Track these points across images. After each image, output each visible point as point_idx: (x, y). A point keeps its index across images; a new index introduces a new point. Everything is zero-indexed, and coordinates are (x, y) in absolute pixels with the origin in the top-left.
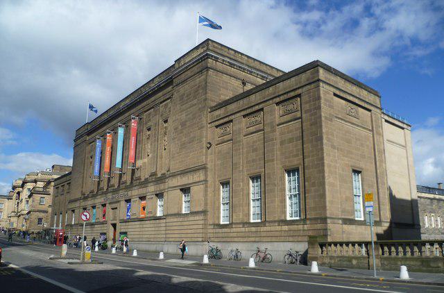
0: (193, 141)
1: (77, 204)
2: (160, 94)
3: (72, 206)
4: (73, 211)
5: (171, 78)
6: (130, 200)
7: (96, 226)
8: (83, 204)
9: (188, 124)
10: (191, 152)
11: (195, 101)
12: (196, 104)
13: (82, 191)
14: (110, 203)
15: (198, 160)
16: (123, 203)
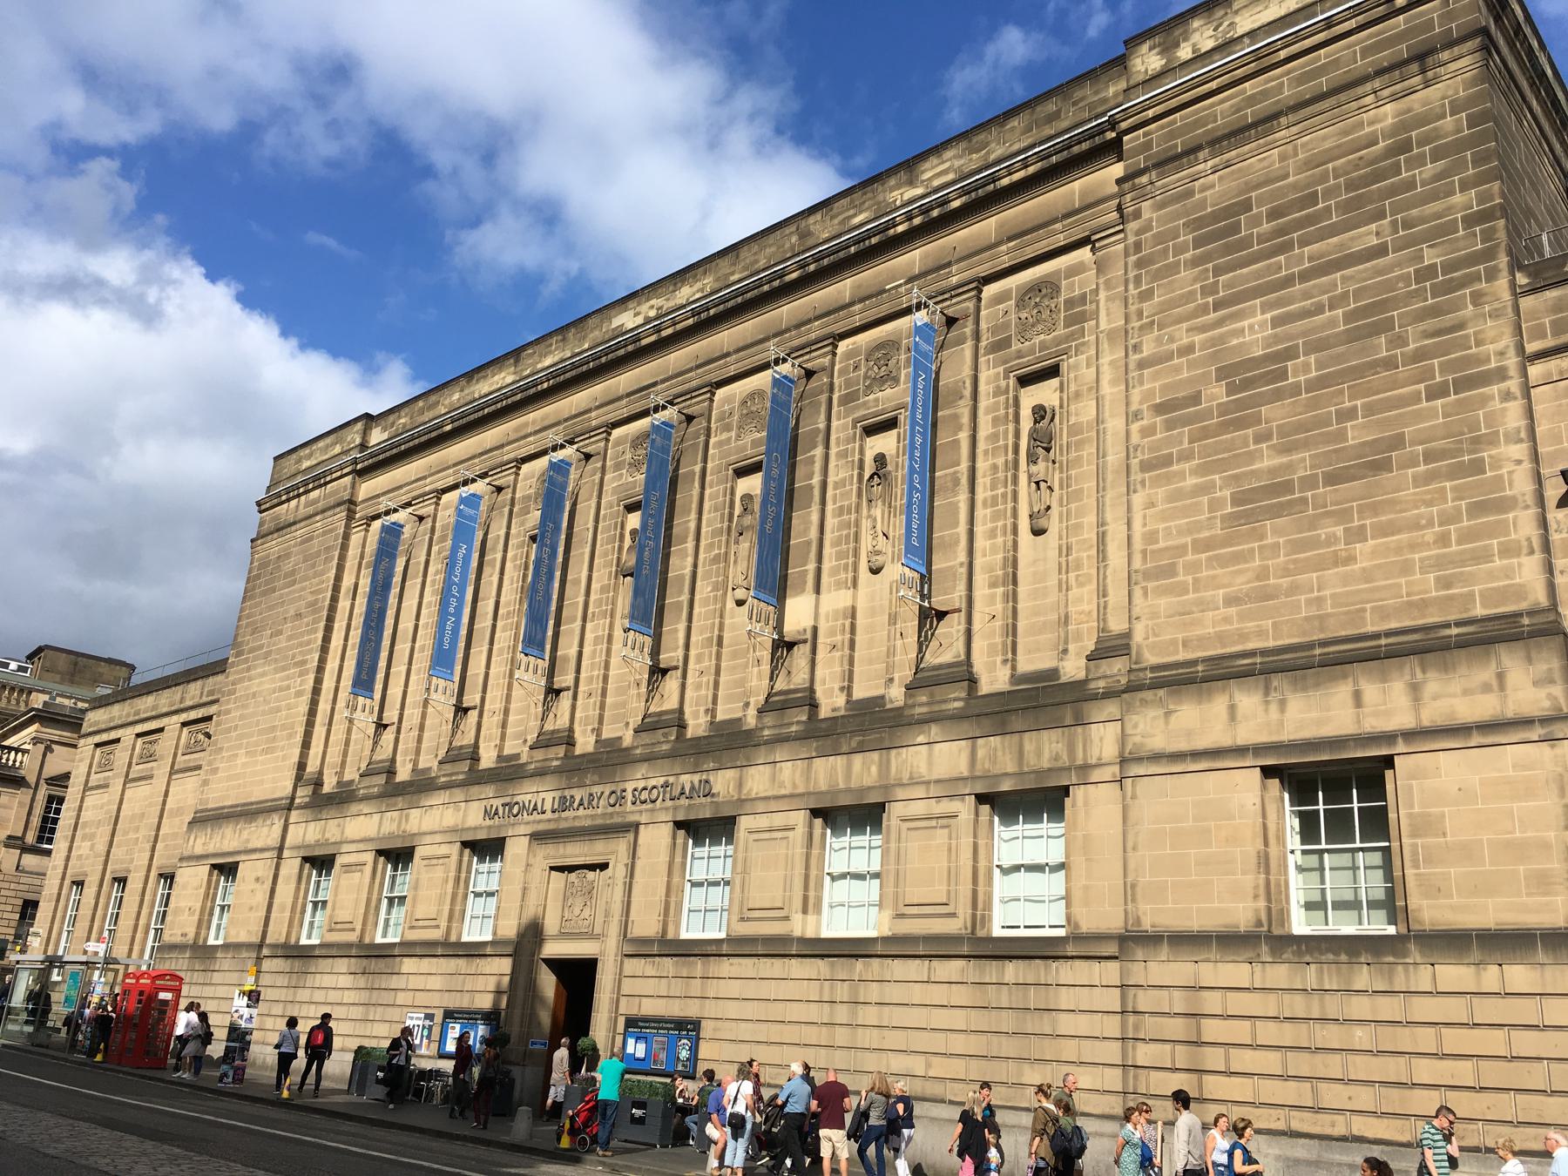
0: (1382, 466)
1: (265, 833)
2: (987, 226)
3: (226, 840)
4: (228, 870)
5: (1112, 124)
6: (881, 807)
7: (408, 965)
8: (307, 832)
9: (1303, 369)
10: (1359, 535)
11: (1367, 236)
12: (1381, 250)
13: (302, 766)
14: (538, 837)
15: (1445, 583)
16: (656, 838)
